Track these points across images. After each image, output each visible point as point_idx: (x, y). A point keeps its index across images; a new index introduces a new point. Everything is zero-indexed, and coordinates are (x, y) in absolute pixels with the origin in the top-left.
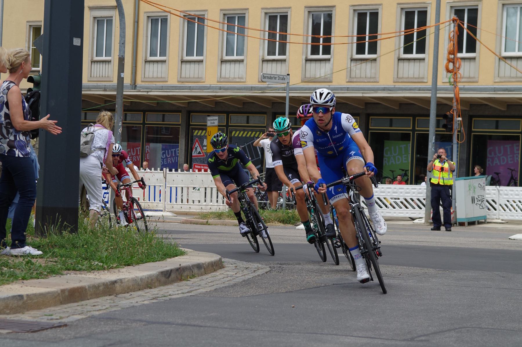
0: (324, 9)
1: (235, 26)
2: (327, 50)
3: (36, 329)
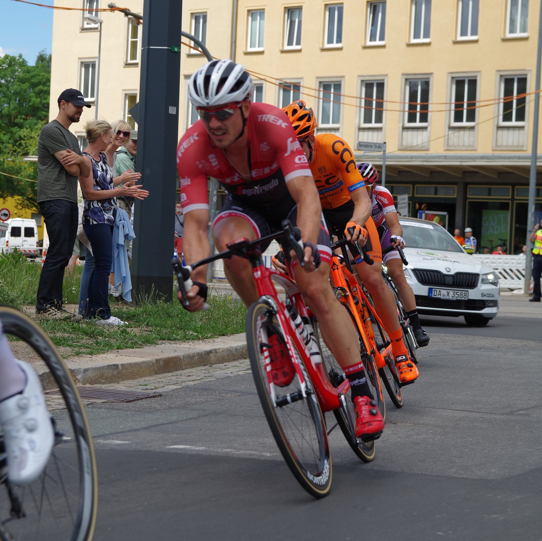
0: (421, 77)
1: (330, 93)
2: (424, 118)
3: (131, 399)
